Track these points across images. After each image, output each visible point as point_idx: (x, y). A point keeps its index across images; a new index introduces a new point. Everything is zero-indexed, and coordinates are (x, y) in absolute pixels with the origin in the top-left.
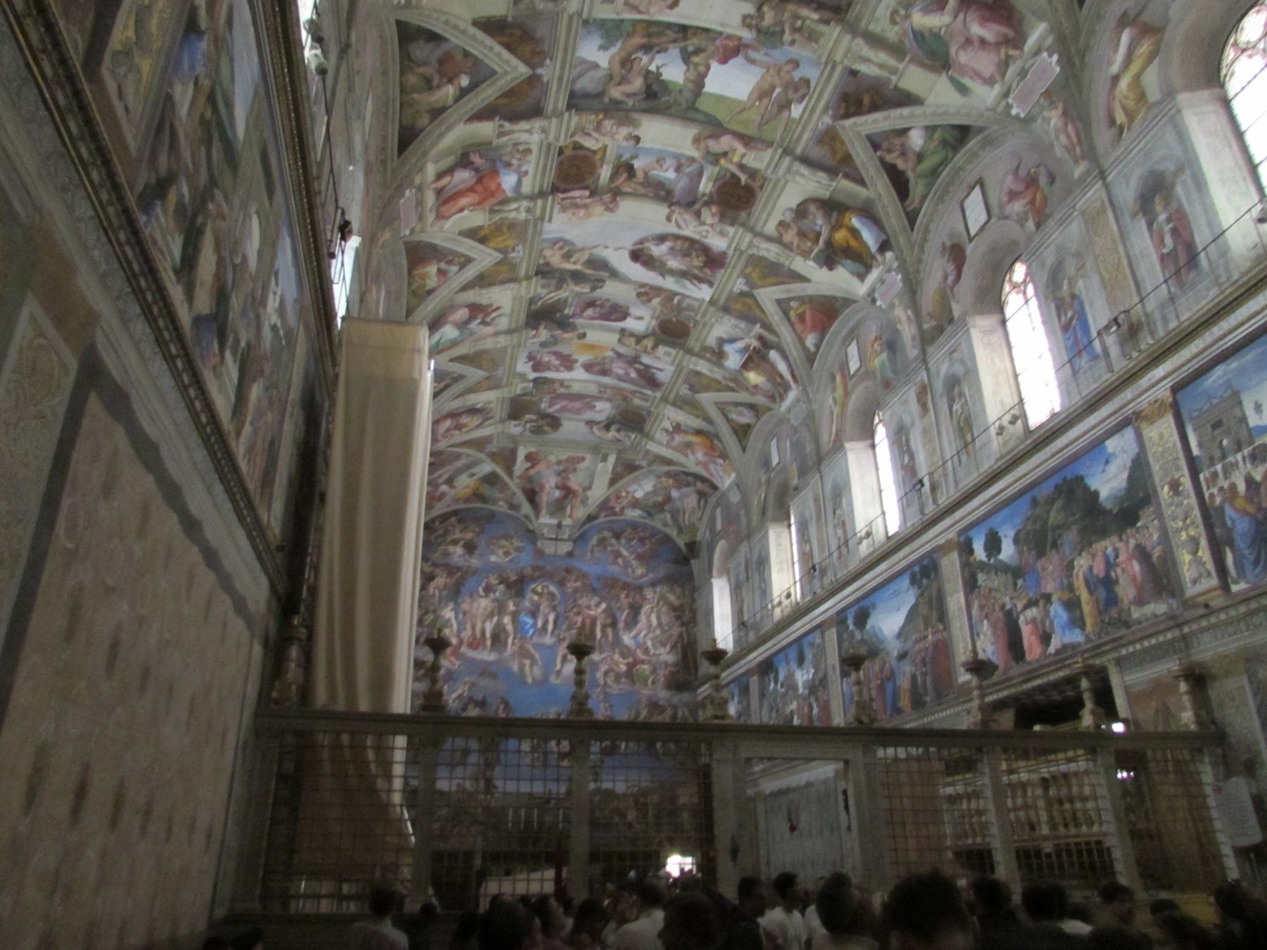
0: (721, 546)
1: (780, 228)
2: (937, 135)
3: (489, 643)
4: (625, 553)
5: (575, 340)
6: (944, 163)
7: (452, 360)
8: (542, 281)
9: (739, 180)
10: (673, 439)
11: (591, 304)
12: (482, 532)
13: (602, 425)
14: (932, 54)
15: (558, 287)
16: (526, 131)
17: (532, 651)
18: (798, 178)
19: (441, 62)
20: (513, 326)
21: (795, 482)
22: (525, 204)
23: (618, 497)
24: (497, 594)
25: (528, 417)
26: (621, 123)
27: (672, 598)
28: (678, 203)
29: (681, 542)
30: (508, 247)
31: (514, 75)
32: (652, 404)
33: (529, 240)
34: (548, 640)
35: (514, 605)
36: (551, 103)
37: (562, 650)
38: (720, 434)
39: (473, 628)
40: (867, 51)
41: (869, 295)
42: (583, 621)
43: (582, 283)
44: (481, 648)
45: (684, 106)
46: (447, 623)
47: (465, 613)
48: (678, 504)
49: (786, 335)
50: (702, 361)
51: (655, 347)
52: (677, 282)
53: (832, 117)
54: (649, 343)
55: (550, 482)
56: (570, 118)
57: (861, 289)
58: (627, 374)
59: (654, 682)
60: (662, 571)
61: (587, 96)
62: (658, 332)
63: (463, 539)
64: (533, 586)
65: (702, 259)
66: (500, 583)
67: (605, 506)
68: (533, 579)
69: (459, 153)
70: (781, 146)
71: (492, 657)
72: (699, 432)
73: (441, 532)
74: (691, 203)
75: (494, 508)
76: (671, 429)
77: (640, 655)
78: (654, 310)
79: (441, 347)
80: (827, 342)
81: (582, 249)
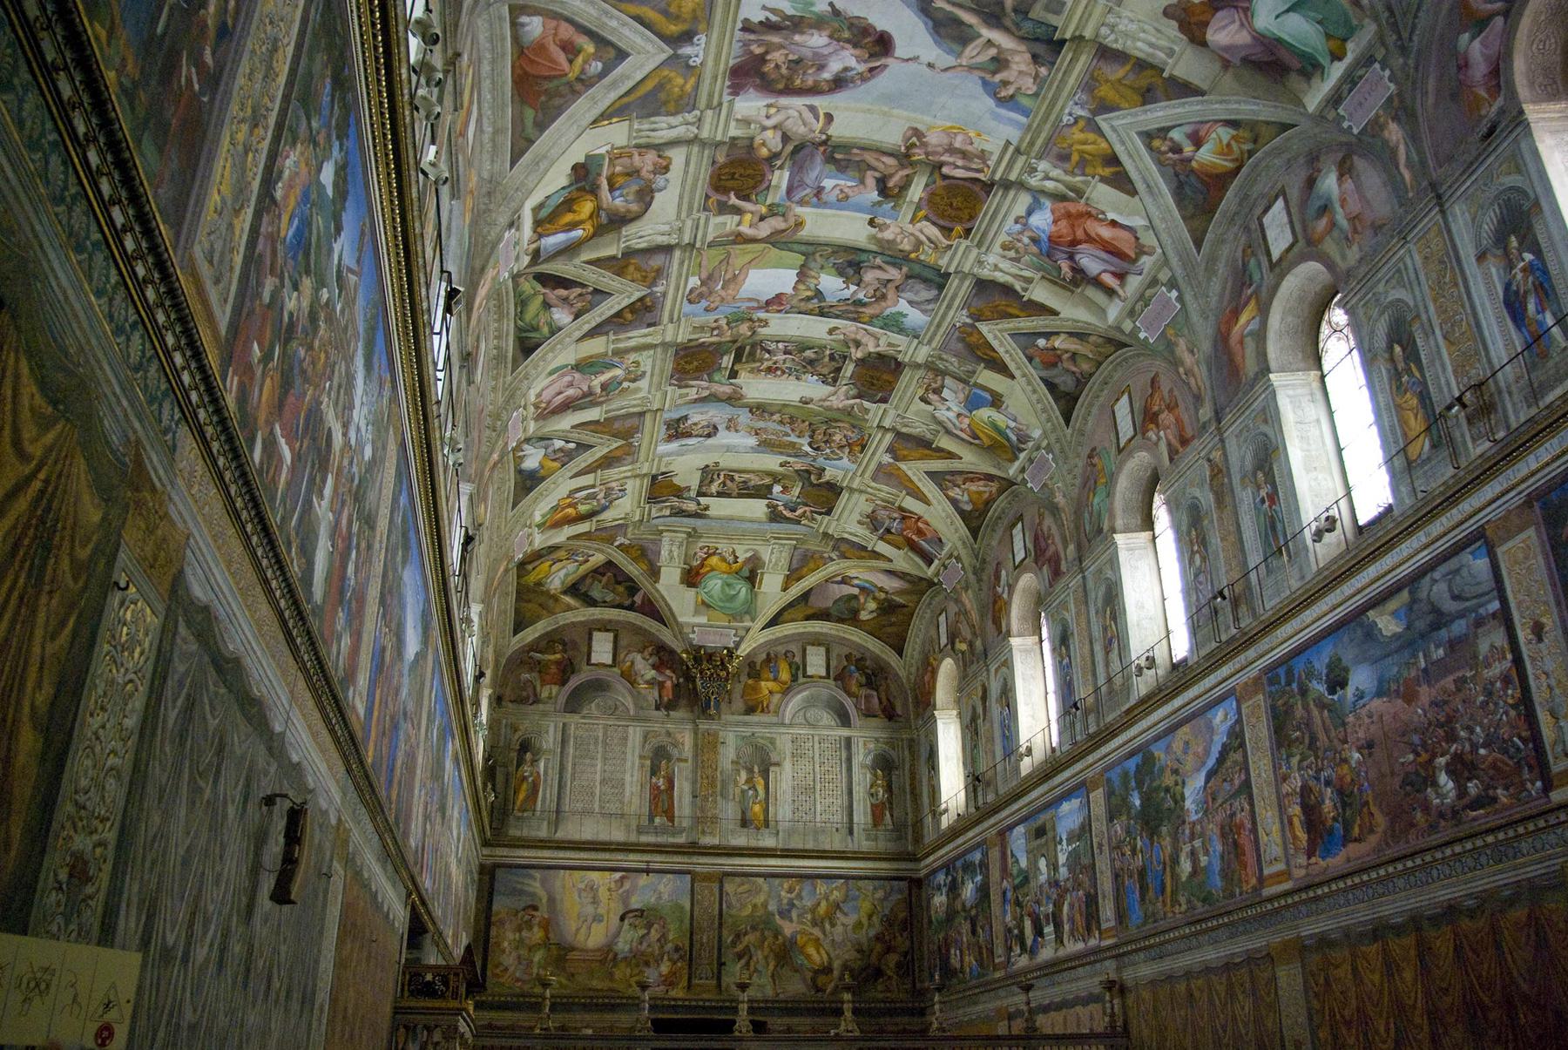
2: (546, 330)
6: (520, 315)
9: (738, 197)
14: (592, 365)
18: (666, 228)
19: (1054, 365)
22: (1033, 182)
28: (817, 145)
30: (1082, 131)
33: (1048, 126)
36: (964, 288)
40: (649, 340)
61: (925, 281)
74: (799, 151)
80: (503, 39)
81: (971, 68)
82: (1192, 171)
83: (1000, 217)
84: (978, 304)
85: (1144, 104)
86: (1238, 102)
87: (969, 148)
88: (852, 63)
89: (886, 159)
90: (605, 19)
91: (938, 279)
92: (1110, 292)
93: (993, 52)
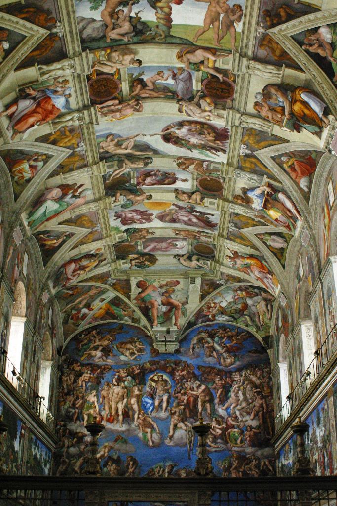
0: (283, 336)
1: (257, 107)
3: (121, 418)
4: (218, 348)
5: (146, 201)
7: (60, 224)
8: (106, 164)
10: (236, 262)
11: (148, 174)
12: (114, 340)
13: (185, 257)
15: (120, 167)
16: (59, 69)
17: (152, 423)
18: (257, 72)
20: (97, 196)
21: (311, 289)
22: (76, 115)
23: (209, 308)
24: (126, 383)
25: (132, 256)
26: (124, 54)
27: (254, 378)
29: (260, 339)
31: (38, 36)
32: (214, 239)
34: (163, 414)
35: (139, 390)
36: (71, 49)
37: (175, 419)
38: (265, 257)
39: (110, 408)
41: (326, 147)
42: (188, 399)
43: (137, 161)
44: (116, 422)
45: (163, 37)
46: (92, 406)
47: (104, 398)
48: (253, 309)
49: (286, 182)
50: (237, 206)
51: (202, 199)
52: (201, 153)
53: (263, 27)
54: (197, 196)
55: (158, 300)
56: (87, 57)
57: (320, 144)
58: (190, 220)
59: (242, 441)
60: (247, 360)
61: (93, 40)
62: (201, 188)
63: (101, 346)
64: (152, 376)
65: (213, 135)
66: (128, 376)
67: (199, 314)
68: (151, 371)
69: (17, 90)
70: (238, 52)
71: (124, 428)
72: (251, 257)
73: (86, 342)
74: (190, 98)
75: (122, 322)
76: (232, 256)
77: (231, 422)
78: (193, 173)
79: (48, 216)
81: (128, 139)
82: (24, 159)
83: (79, 93)
84: (57, 45)
85: (60, 164)
86: (35, 188)
87: (112, 115)
88: (177, 132)
89: (147, 95)
90: (279, 173)
91: (88, 45)
92: (7, 107)
93: (123, 147)
